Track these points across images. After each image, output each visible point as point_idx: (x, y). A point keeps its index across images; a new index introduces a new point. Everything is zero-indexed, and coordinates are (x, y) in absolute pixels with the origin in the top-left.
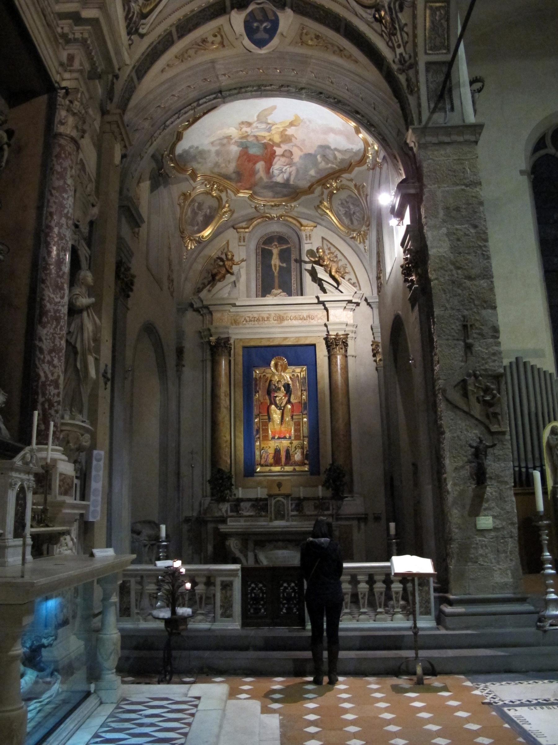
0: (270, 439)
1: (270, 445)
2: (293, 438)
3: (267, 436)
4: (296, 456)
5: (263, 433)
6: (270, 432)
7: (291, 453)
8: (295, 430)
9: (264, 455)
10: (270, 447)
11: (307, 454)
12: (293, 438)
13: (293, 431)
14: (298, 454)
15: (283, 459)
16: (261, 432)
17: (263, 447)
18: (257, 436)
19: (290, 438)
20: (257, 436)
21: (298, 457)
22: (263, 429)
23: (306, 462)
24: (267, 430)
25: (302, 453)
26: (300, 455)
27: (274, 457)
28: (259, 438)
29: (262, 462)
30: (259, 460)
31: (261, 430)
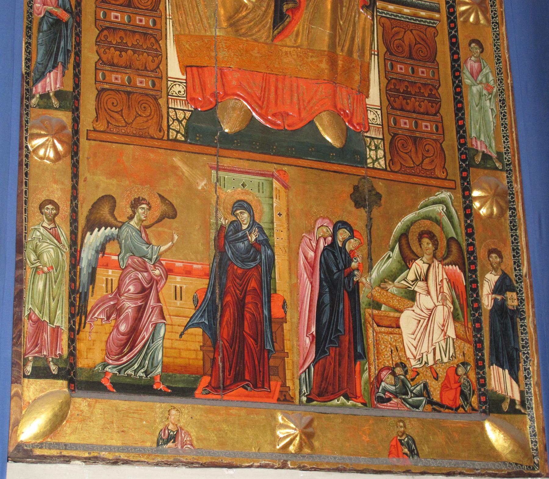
0: (177, 131)
1: (168, 187)
2: (377, 157)
3: (153, 98)
4: (408, 320)
5: (103, 63)
6: (174, 69)
7: (368, 282)
8: (397, 93)
9: (107, 276)
10: (171, 213)
11: (500, 310)
12: (377, 157)
13: (374, 97)
14: (424, 301)
15: (298, 338)
16: (90, 56)
17: (109, 200)
18: (52, 82)
19: (351, 153)
20: (52, 82)
21: (423, 329)
22: (106, 30)
23: (499, 380)
24: (153, 38)
25: (466, 301)
26: (442, 313)
27: (209, 312)
28: (70, 100)
29: (93, 353)
30: (61, 320)
31: (89, 35)
